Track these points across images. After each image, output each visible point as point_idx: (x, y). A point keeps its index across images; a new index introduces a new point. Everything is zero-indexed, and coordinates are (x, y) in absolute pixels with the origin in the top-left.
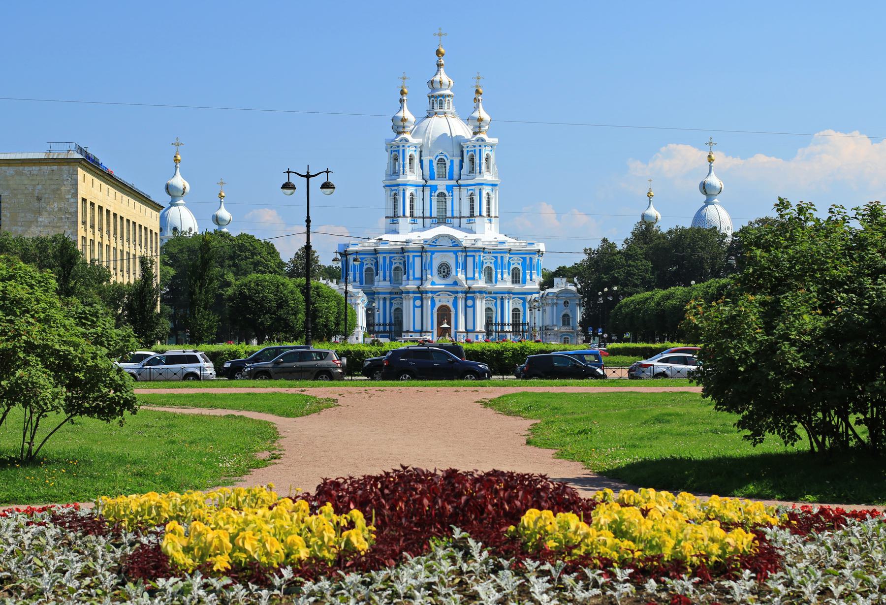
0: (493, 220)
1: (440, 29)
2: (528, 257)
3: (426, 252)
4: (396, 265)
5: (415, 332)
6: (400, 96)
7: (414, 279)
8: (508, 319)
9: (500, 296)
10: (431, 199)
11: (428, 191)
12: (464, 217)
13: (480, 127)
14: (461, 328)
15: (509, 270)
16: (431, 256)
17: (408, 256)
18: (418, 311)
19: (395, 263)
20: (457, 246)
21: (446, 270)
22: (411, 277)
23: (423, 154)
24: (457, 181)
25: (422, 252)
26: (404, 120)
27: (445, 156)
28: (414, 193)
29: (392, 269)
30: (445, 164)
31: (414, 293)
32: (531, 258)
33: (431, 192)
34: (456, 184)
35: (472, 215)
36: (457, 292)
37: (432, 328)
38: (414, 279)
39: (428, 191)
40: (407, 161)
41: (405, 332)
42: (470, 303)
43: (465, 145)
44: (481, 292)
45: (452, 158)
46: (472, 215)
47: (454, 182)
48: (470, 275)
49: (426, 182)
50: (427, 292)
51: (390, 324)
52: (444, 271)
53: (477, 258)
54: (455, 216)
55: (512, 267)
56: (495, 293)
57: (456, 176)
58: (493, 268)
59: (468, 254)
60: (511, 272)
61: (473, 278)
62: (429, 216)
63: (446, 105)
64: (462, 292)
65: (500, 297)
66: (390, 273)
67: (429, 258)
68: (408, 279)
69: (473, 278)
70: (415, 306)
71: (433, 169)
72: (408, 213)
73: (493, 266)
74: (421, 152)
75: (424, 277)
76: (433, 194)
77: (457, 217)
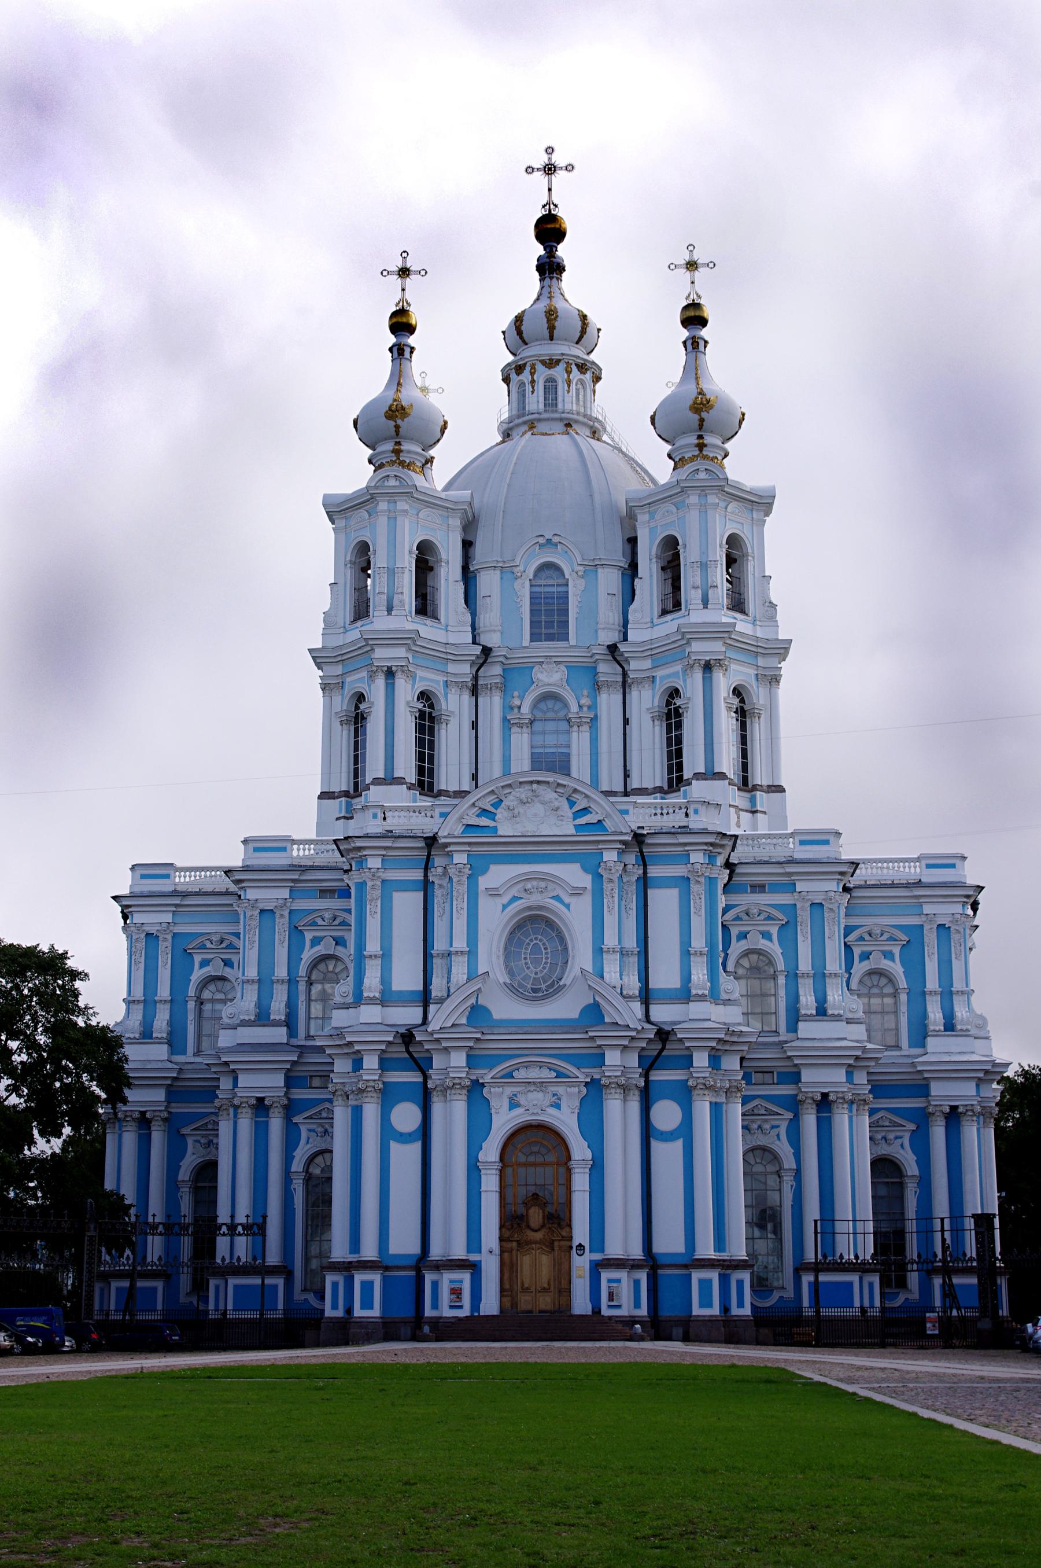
1: (550, 150)
4: (320, 950)
6: (392, 339)
12: (642, 792)
13: (700, 437)
28: (439, 690)
29: (302, 971)
35: (676, 780)
46: (676, 780)
58: (781, 965)
66: (291, 982)
70: (388, 1133)
72: (407, 767)
74: (467, 545)
75: (437, 988)
76: (517, 702)
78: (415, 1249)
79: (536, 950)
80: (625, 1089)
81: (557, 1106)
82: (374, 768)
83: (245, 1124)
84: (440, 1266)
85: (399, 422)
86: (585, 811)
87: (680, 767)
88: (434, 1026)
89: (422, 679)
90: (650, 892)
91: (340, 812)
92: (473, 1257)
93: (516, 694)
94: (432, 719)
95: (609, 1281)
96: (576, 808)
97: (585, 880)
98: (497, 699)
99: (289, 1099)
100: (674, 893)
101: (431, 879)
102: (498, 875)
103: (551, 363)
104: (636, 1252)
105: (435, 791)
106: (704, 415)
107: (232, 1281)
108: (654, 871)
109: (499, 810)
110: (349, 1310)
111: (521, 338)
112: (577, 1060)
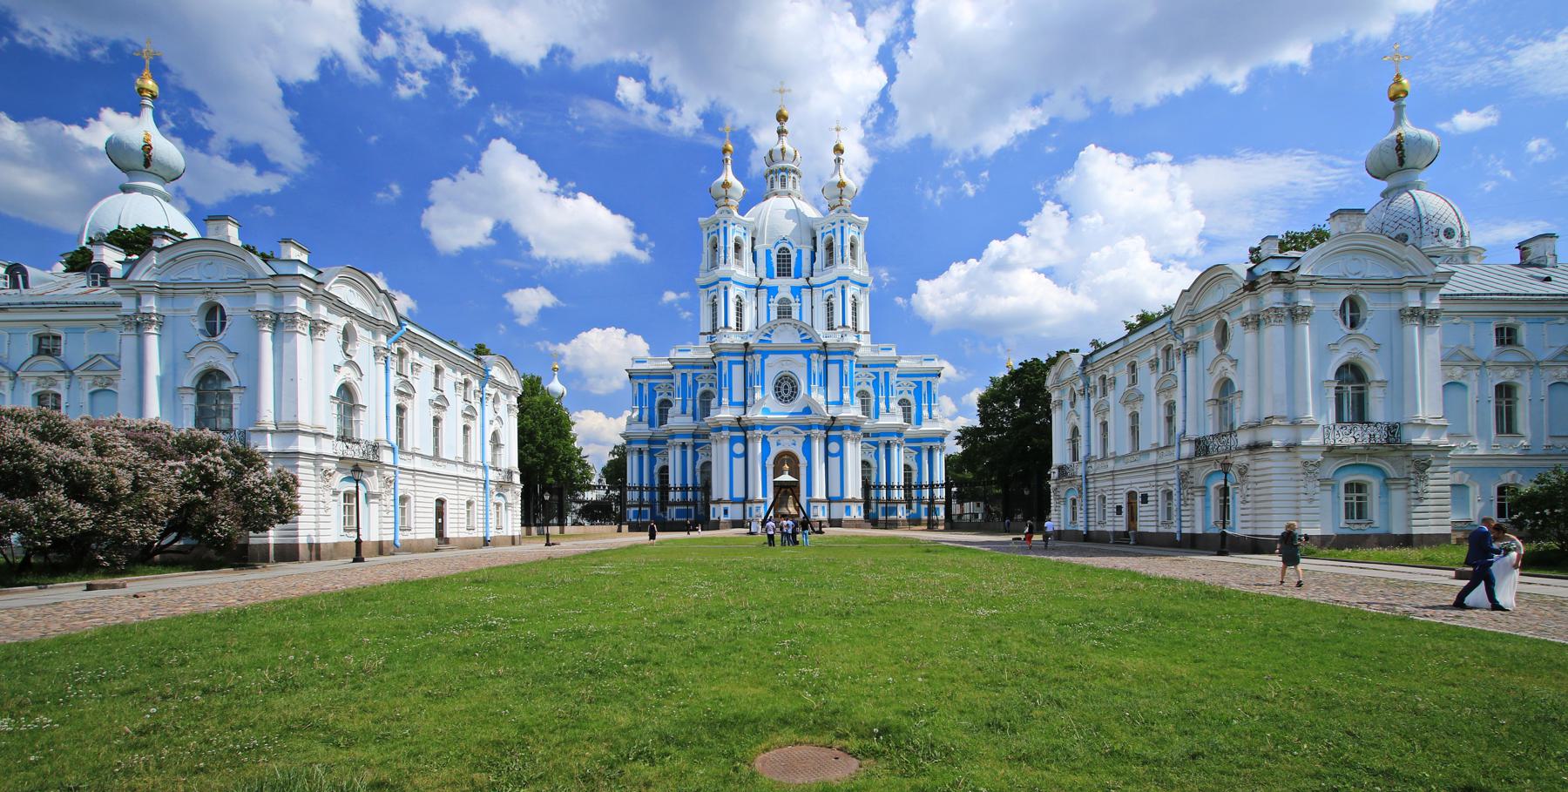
0: (862, 336)
2: (924, 380)
4: (705, 388)
5: (733, 501)
7: (731, 403)
8: (898, 478)
9: (885, 439)
11: (763, 293)
14: (819, 493)
16: (762, 361)
17: (720, 363)
18: (739, 463)
19: (702, 385)
20: (810, 340)
21: (790, 389)
22: (725, 400)
23: (756, 241)
24: (808, 279)
25: (745, 355)
26: (726, 185)
27: (790, 243)
30: (789, 256)
31: (731, 429)
32: (929, 383)
33: (769, 298)
36: (810, 427)
38: (731, 403)
39: (763, 293)
40: (731, 245)
41: (714, 502)
42: (834, 447)
43: (815, 227)
44: (855, 428)
45: (799, 247)
47: (801, 282)
49: (761, 279)
50: (754, 428)
51: (695, 489)
52: (786, 388)
53: (846, 366)
56: (877, 435)
57: (805, 274)
59: (830, 358)
61: (840, 403)
63: (790, 184)
64: (820, 427)
65: (881, 441)
66: (694, 401)
67: (758, 365)
68: (720, 404)
69: (840, 403)
70: (732, 455)
71: (771, 264)
72: (732, 323)
73: (870, 390)
74: (753, 239)
78: (742, 495)
79: (786, 387)
83: (678, 452)
84: (751, 502)
86: (805, 334)
88: (749, 415)
97: (805, 361)
98: (765, 298)
100: (837, 366)
102: (771, 359)
103: (784, 170)
107: (675, 508)
112: (802, 427)
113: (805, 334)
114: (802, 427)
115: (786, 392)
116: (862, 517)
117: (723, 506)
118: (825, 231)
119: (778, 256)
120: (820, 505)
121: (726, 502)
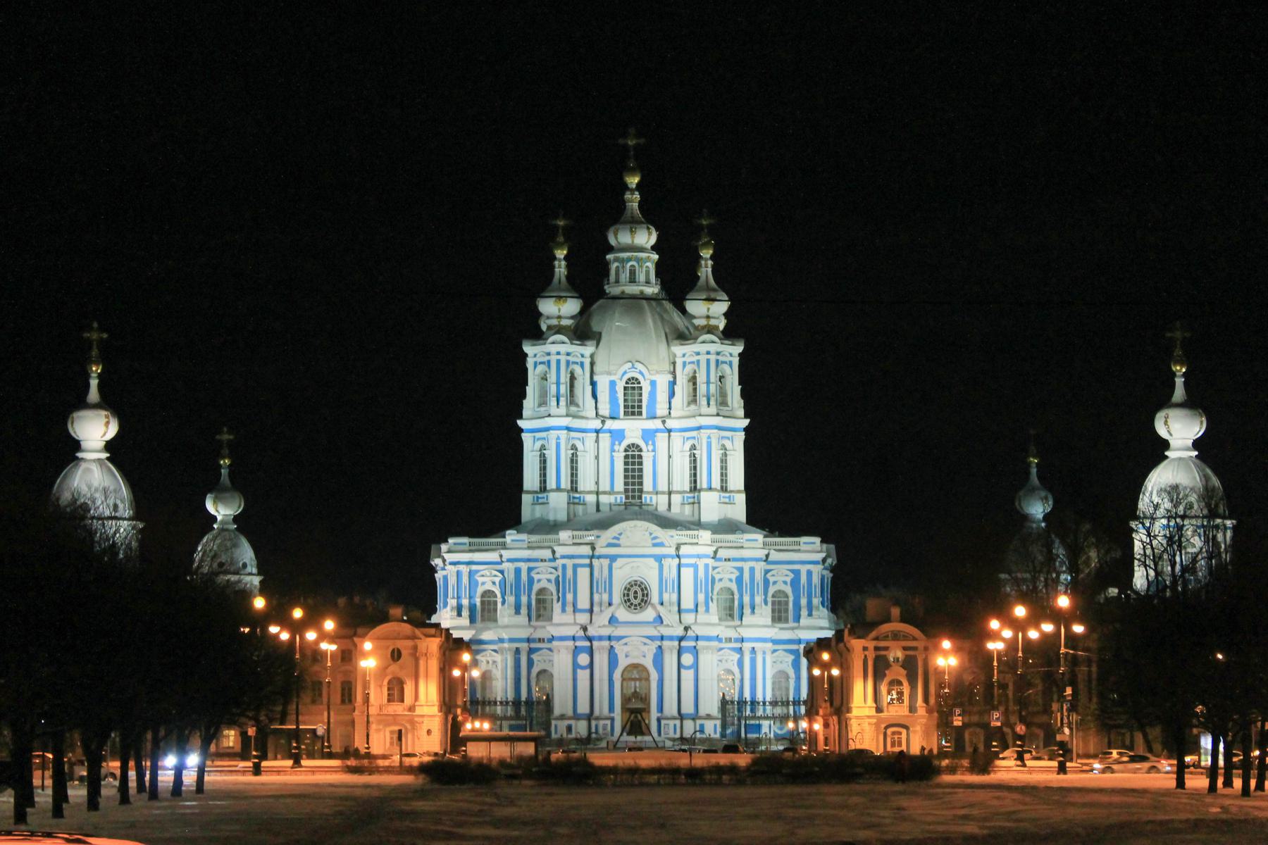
3: (599, 557)
5: (577, 717)
10: (612, 457)
11: (605, 439)
14: (670, 708)
15: (766, 593)
17: (564, 567)
18: (583, 675)
21: (640, 595)
27: (641, 373)
30: (641, 388)
33: (613, 444)
34: (661, 426)
35: (694, 488)
37: (611, 709)
39: (605, 439)
41: (557, 719)
42: (687, 659)
47: (657, 424)
48: (687, 603)
54: (660, 489)
55: (772, 590)
60: (770, 600)
62: (608, 489)
66: (529, 596)
70: (576, 666)
74: (592, 364)
75: (596, 609)
77: (663, 493)
79: (636, 592)
80: (671, 650)
81: (644, 656)
82: (551, 483)
84: (597, 719)
85: (561, 307)
87: (695, 482)
88: (597, 625)
89: (573, 438)
90: (682, 569)
91: (534, 500)
92: (612, 715)
93: (617, 443)
94: (577, 456)
95: (665, 724)
96: (653, 536)
97: (656, 565)
99: (530, 649)
101: (593, 563)
102: (620, 562)
104: (675, 713)
105: (579, 490)
106: (710, 306)
108: (684, 561)
109: (621, 537)
110: (562, 736)
111: (617, 240)
113: (655, 538)
114: (651, 638)
115: (636, 598)
116: (718, 736)
117: (567, 722)
118: (688, 359)
119: (625, 388)
120: (671, 723)
121: (569, 718)
